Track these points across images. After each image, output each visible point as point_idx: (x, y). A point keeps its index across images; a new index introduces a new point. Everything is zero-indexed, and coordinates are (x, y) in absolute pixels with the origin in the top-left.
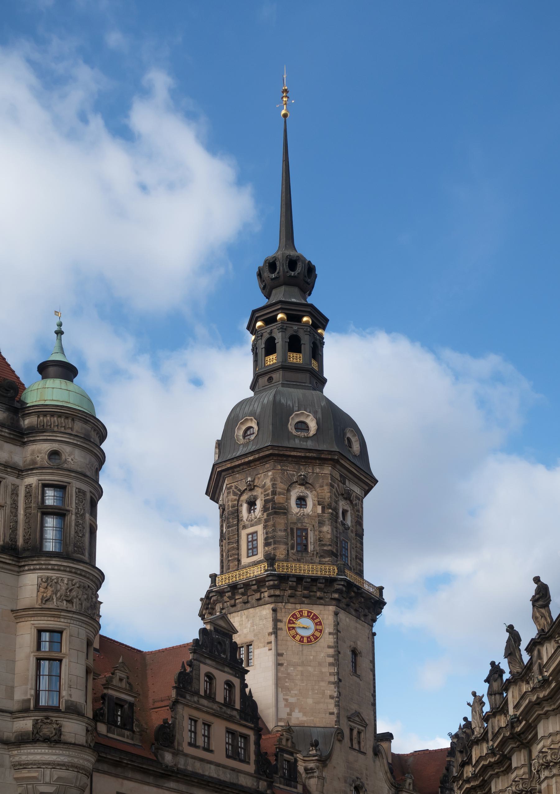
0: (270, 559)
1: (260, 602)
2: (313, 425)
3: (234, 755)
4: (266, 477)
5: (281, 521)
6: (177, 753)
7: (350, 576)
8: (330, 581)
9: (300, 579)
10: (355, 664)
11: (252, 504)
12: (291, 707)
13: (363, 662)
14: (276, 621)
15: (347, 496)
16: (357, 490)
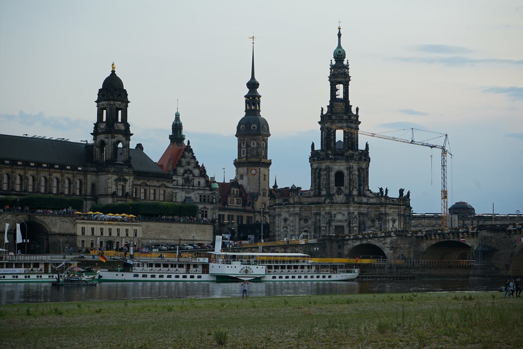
0: (247, 157)
1: (244, 166)
2: (256, 127)
3: (238, 203)
4: (247, 139)
5: (249, 149)
6: (228, 205)
7: (263, 160)
8: (259, 163)
9: (252, 162)
10: (265, 178)
11: (244, 143)
12: (251, 189)
13: (267, 177)
14: (248, 171)
15: (264, 140)
16: (266, 138)
